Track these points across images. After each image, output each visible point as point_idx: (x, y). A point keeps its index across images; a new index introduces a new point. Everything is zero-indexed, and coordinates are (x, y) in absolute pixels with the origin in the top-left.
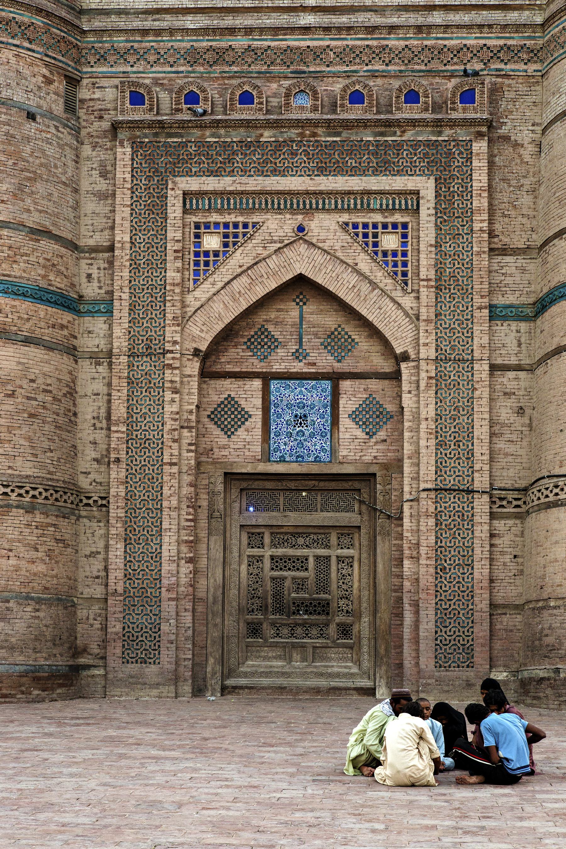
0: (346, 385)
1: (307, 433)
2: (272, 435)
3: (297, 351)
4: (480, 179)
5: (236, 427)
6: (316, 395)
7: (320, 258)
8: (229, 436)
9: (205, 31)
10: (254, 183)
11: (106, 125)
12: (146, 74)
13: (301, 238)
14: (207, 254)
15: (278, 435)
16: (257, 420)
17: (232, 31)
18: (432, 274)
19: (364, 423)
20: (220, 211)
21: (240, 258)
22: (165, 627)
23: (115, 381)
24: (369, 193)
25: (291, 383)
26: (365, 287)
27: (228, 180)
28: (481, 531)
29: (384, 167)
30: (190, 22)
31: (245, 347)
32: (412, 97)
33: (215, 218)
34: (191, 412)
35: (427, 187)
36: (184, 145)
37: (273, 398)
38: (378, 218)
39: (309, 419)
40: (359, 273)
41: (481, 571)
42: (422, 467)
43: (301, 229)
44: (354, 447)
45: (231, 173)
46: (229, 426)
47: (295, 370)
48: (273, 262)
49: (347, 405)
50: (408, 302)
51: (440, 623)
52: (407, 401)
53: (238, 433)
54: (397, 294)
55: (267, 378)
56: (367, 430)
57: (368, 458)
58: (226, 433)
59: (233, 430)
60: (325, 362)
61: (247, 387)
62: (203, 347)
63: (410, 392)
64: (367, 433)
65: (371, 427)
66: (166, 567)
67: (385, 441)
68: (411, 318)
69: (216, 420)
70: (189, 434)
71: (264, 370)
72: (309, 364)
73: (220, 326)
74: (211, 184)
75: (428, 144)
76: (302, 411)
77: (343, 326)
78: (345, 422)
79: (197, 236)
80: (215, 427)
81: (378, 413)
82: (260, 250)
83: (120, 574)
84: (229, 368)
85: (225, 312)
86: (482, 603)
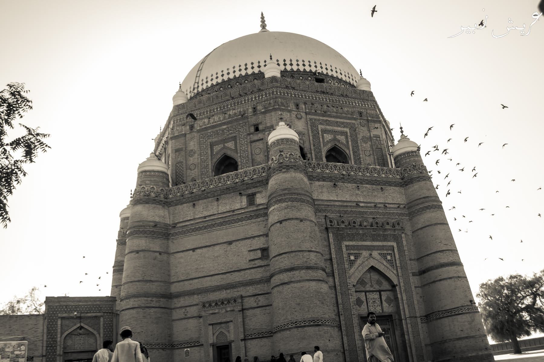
0: (382, 293)
4: (405, 243)
7: (376, 262)
9: (342, 206)
10: (360, 243)
11: (324, 228)
12: (331, 216)
14: (352, 261)
16: (365, 303)
17: (347, 206)
20: (353, 250)
21: (359, 262)
22: (359, 358)
23: (338, 294)
24: (383, 246)
26: (386, 268)
27: (354, 242)
28: (420, 327)
29: (385, 240)
30: (337, 203)
32: (388, 224)
33: (352, 252)
35: (395, 244)
36: (343, 234)
38: (385, 252)
41: (422, 336)
42: (406, 312)
43: (371, 255)
44: (388, 309)
45: (355, 241)
48: (366, 263)
49: (384, 298)
50: (395, 272)
51: (416, 351)
52: (399, 296)
54: (393, 270)
55: (366, 292)
57: (390, 311)
60: (377, 288)
66: (357, 342)
73: (358, 279)
74: (351, 243)
75: (393, 235)
78: (384, 302)
79: (349, 256)
83: (347, 345)
84: (357, 290)
85: (358, 275)
86: (423, 345)
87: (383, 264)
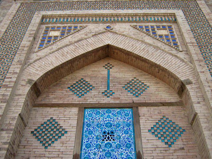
0: (143, 110)
1: (114, 145)
2: (84, 147)
3: (106, 91)
5: (53, 140)
6: (120, 118)
8: (46, 147)
13: (109, 31)
15: (88, 146)
18: (194, 40)
19: (162, 135)
25: (101, 111)
31: (68, 90)
34: (13, 119)
37: (86, 120)
39: (115, 134)
40: (146, 43)
46: (48, 140)
47: (104, 102)
53: (54, 145)
54: (174, 52)
55: (83, 108)
56: (166, 141)
58: (44, 144)
59: (50, 142)
60: (127, 97)
61: (66, 113)
62: (35, 78)
63: (199, 103)
64: (166, 143)
65: (168, 138)
67: (183, 149)
68: (186, 63)
69: (38, 135)
70: (7, 135)
71: (81, 102)
72: (114, 98)
76: (110, 129)
77: (137, 78)
80: (36, 140)
81: (172, 128)
82: (83, 36)
84: (55, 101)
87: (143, 42)
